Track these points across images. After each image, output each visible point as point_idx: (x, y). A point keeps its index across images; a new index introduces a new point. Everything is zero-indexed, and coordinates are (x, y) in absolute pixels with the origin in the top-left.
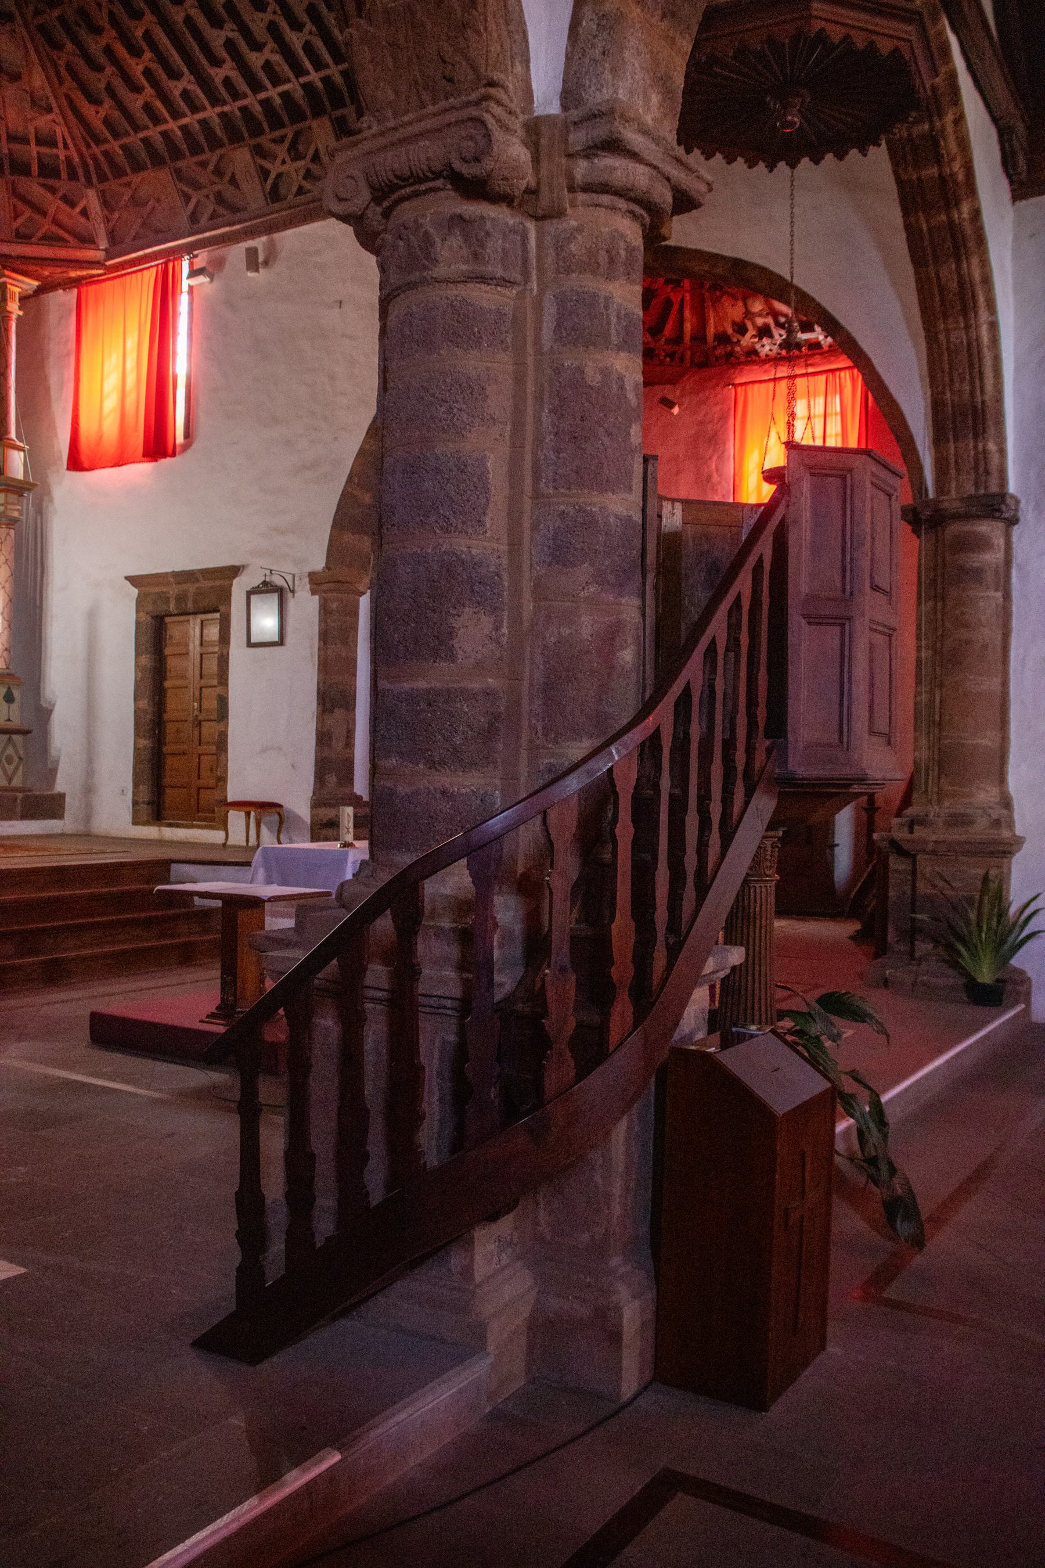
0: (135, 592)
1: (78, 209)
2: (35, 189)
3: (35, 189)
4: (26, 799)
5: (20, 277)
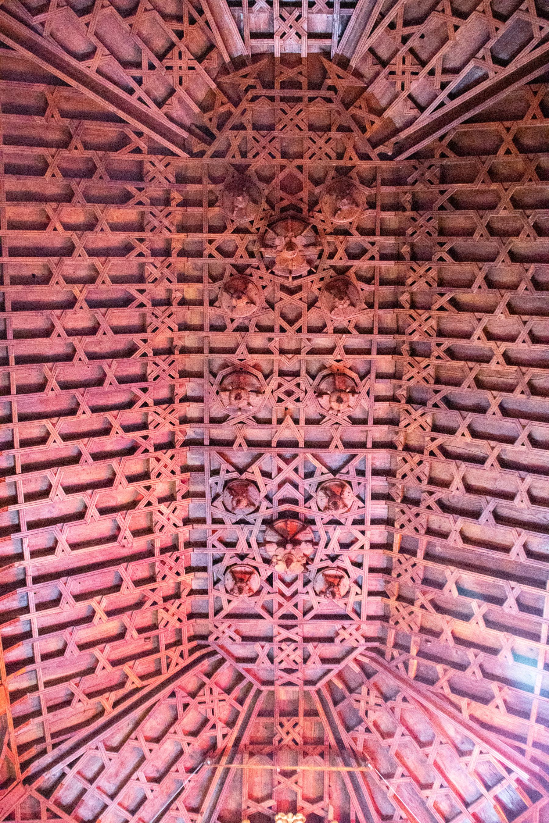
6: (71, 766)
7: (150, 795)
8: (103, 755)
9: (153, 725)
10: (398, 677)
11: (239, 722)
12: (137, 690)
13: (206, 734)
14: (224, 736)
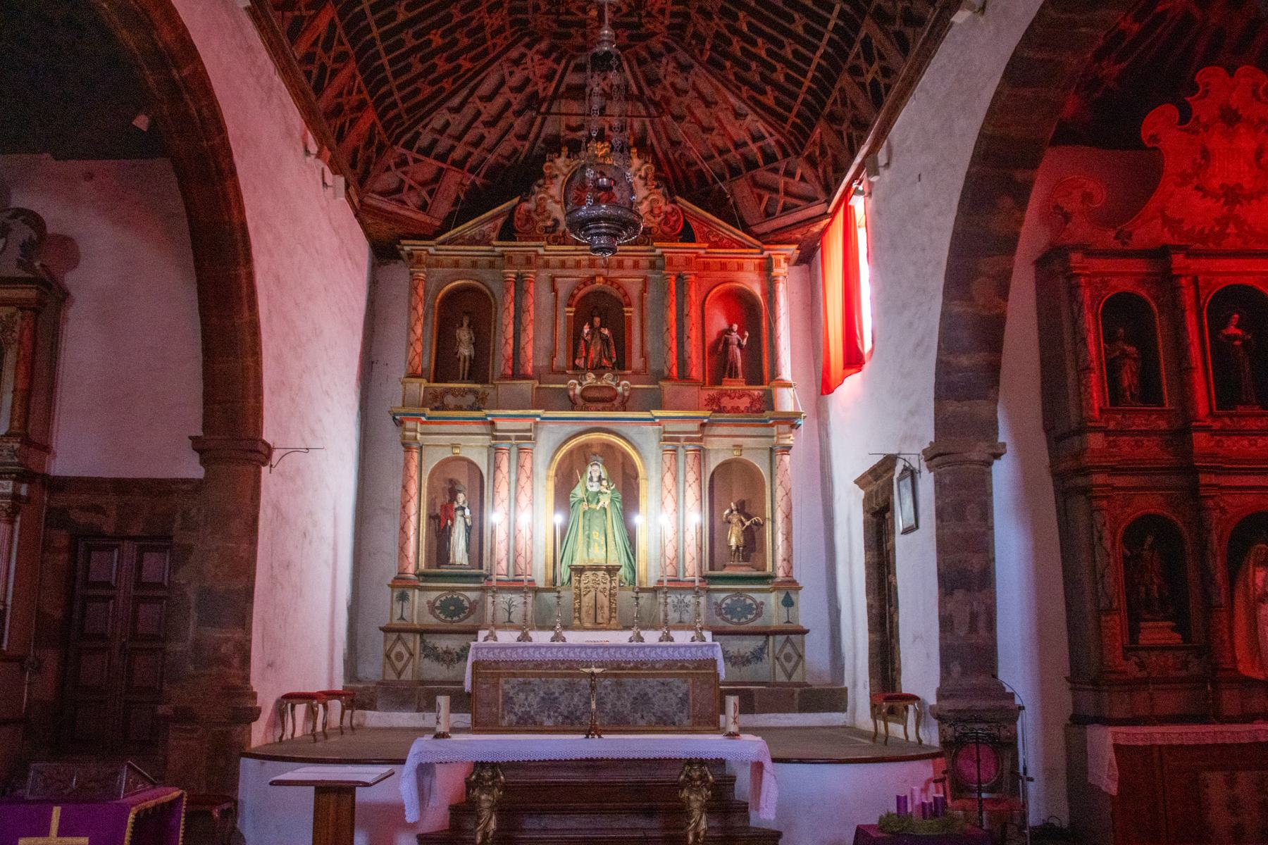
0: (862, 493)
1: (797, 178)
2: (763, 175)
3: (763, 175)
4: (801, 693)
5: (778, 247)
6: (424, 127)
7: (486, 134)
8: (448, 116)
9: (485, 89)
10: (693, 57)
11: (557, 77)
12: (469, 70)
13: (529, 89)
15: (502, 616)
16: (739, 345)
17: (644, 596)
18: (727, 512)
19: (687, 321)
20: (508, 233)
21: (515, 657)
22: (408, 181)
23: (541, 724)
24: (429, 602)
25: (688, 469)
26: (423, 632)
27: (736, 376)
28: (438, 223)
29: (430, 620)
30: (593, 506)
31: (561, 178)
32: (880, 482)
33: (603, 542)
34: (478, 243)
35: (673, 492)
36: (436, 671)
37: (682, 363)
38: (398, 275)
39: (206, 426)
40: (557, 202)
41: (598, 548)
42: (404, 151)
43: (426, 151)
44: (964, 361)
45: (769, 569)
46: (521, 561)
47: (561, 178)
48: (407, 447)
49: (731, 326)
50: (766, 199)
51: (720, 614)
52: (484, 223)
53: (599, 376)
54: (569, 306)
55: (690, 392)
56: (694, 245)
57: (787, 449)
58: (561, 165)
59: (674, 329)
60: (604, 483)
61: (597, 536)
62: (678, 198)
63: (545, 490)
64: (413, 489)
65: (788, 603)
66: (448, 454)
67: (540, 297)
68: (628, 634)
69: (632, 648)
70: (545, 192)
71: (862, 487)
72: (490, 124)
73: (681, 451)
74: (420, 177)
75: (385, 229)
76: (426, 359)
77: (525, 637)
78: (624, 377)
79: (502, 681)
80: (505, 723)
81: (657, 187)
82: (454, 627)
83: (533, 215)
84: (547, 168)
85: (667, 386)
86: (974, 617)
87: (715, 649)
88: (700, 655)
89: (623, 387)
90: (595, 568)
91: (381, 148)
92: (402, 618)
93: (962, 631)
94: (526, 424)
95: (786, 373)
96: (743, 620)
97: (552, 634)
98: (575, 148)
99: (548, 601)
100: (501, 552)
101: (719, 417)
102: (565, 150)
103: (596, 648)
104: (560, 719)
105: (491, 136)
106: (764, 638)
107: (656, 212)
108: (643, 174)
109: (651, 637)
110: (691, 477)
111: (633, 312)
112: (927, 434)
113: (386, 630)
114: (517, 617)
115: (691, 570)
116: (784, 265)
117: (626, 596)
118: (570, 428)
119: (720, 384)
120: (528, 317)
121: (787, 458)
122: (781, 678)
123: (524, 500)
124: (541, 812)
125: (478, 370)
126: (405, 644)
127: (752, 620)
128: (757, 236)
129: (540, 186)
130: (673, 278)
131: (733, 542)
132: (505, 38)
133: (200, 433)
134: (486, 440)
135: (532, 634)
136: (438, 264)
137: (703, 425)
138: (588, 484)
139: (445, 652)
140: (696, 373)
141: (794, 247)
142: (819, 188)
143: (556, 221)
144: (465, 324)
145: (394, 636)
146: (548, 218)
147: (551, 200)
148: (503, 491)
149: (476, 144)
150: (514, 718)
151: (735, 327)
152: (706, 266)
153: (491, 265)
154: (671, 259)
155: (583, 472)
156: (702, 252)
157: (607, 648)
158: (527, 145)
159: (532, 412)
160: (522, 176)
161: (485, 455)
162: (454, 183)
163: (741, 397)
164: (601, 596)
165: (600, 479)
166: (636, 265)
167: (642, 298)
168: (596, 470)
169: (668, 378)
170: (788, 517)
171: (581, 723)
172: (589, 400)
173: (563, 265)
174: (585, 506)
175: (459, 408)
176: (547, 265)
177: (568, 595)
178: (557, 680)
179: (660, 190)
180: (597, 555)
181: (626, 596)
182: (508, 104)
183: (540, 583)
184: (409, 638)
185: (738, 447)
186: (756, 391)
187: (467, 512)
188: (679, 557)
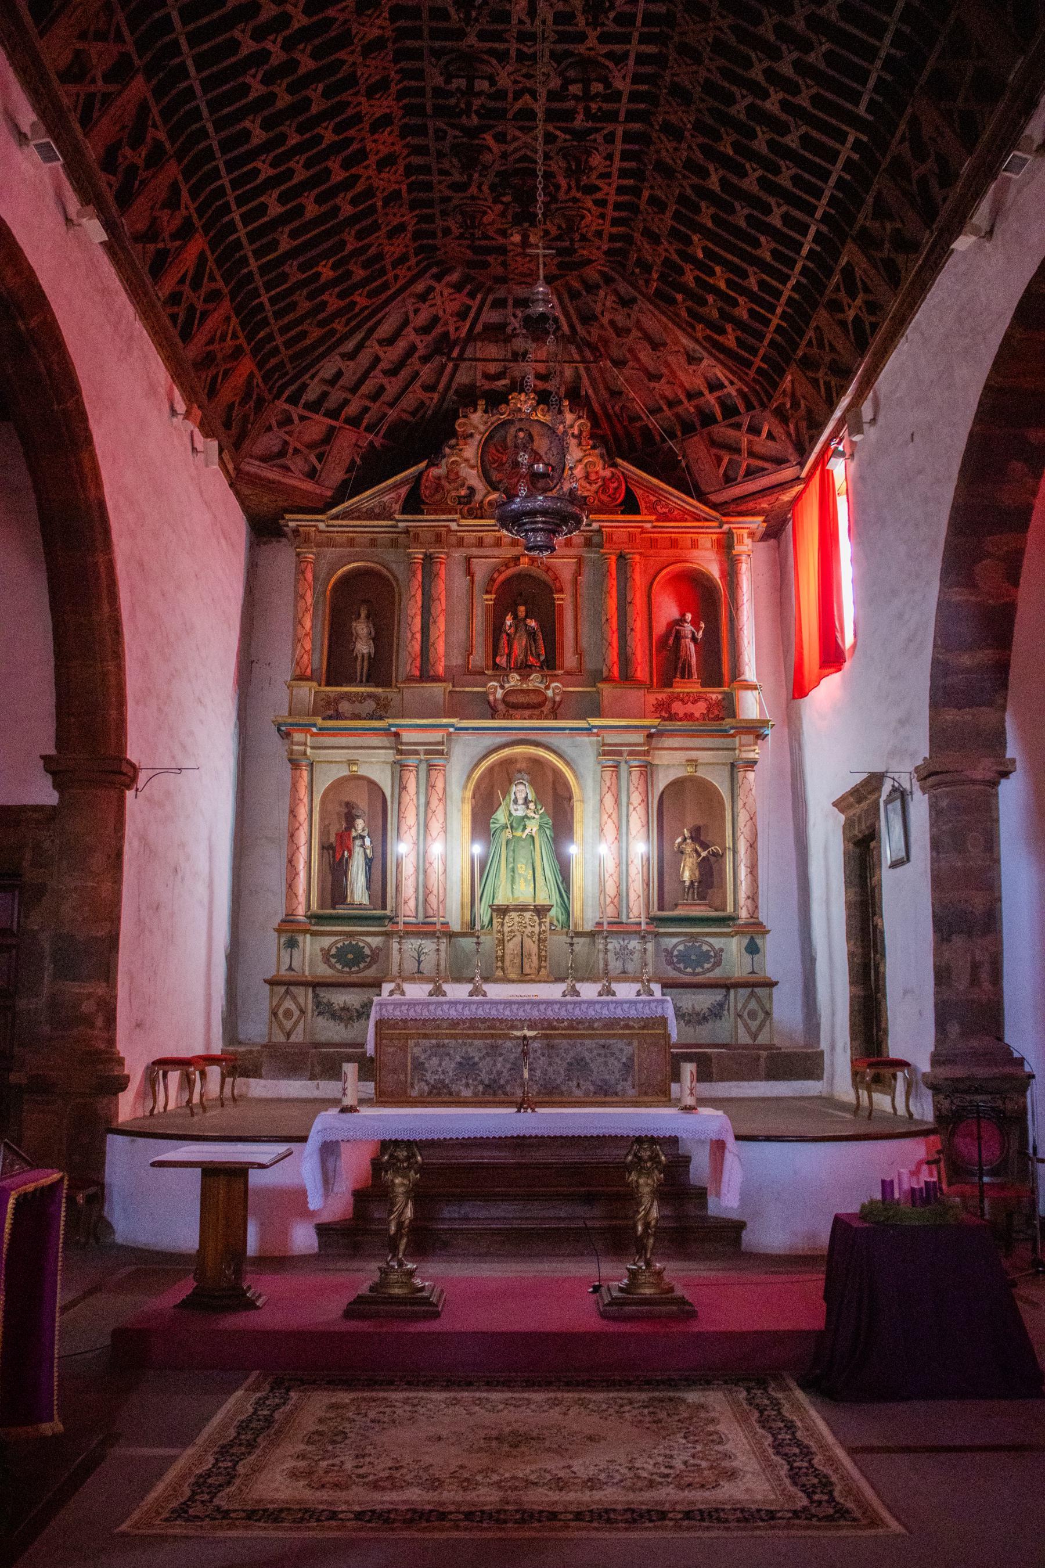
0: (842, 817)
1: (764, 434)
2: (722, 431)
3: (722, 431)
5: (741, 519)
6: (312, 378)
7: (388, 387)
9: (384, 330)
10: (636, 288)
11: (472, 315)
12: (366, 307)
13: (438, 330)
14: (457, 329)
15: (410, 966)
16: (694, 639)
17: (580, 941)
18: (679, 840)
19: (630, 609)
20: (413, 504)
21: (426, 1014)
22: (293, 443)
23: (458, 1094)
24: (322, 950)
25: (632, 789)
26: (316, 985)
27: (690, 676)
28: (329, 493)
29: (324, 971)
30: (518, 833)
31: (478, 437)
32: (862, 804)
33: (530, 877)
34: (377, 517)
35: (614, 816)
36: (331, 1031)
37: (625, 660)
38: (282, 559)
39: (58, 746)
40: (472, 467)
41: (523, 884)
42: (286, 406)
43: (314, 406)
44: (966, 660)
45: (730, 909)
46: (433, 900)
47: (478, 437)
48: (295, 764)
49: (683, 615)
50: (726, 459)
51: (670, 963)
52: (386, 493)
53: (524, 678)
54: (488, 592)
55: (634, 697)
56: (638, 518)
57: (751, 764)
58: (478, 420)
59: (614, 620)
60: (532, 806)
61: (523, 869)
62: (619, 461)
63: (460, 815)
64: (303, 813)
65: (753, 949)
66: (345, 773)
67: (452, 583)
68: (562, 987)
69: (567, 1003)
70: (457, 455)
71: (842, 811)
72: (392, 372)
73: (624, 767)
74: (306, 438)
75: (266, 502)
76: (316, 657)
77: (438, 991)
78: (555, 678)
79: (411, 1043)
80: (415, 1093)
81: (594, 447)
82: (354, 978)
83: (444, 482)
84: (459, 425)
85: (606, 688)
86: (975, 967)
87: (665, 1005)
88: (647, 1013)
89: (554, 690)
90: (522, 909)
91: (260, 402)
92: (290, 968)
93: (962, 985)
94: (437, 736)
95: (750, 673)
96: (699, 970)
97: (470, 987)
98: (496, 400)
99: (466, 947)
100: (409, 889)
101: (669, 725)
102: (482, 403)
103: (522, 1004)
104: (481, 1088)
105: (392, 387)
106: (724, 991)
107: (593, 477)
108: (576, 432)
109: (589, 991)
110: (636, 798)
111: (565, 600)
112: (922, 749)
113: (272, 983)
114: (428, 967)
115: (636, 910)
116: (747, 541)
117: (558, 942)
118: (489, 740)
119: (671, 686)
120: (439, 607)
121: (751, 775)
122: (744, 1038)
123: (435, 826)
124: (461, 1199)
125: (379, 670)
126: (294, 998)
127: (710, 970)
128: (714, 506)
129: (452, 447)
130: (614, 557)
131: (687, 876)
132: (409, 269)
133: (52, 752)
134: (390, 755)
135: (445, 987)
136: (330, 543)
137: (650, 736)
138: (512, 807)
139: (343, 1009)
140: (641, 672)
141: (761, 519)
142: (790, 450)
143: (472, 490)
144: (363, 614)
145: (282, 989)
146: (462, 486)
147: (465, 462)
148: (410, 818)
149: (375, 397)
150: (426, 1088)
151: (689, 616)
152: (653, 543)
153: (394, 544)
154: (610, 535)
155: (506, 793)
156: (649, 525)
157: (536, 1003)
158: (436, 396)
159: (445, 721)
160: (426, 436)
161: (389, 773)
162: (347, 446)
163: (694, 702)
164: (528, 942)
165: (526, 801)
166: (568, 543)
167: (575, 582)
168: (521, 790)
169: (607, 680)
170: (753, 846)
171: (505, 1094)
172: (512, 706)
173: (480, 543)
174: (508, 834)
175: (357, 717)
176: (461, 543)
177: (488, 941)
178: (476, 1042)
179: (597, 451)
180: (524, 893)
181: (558, 942)
182: (412, 349)
183: (456, 927)
184: (299, 991)
185: (693, 762)
186: (715, 695)
187: (367, 841)
188: (621, 896)
